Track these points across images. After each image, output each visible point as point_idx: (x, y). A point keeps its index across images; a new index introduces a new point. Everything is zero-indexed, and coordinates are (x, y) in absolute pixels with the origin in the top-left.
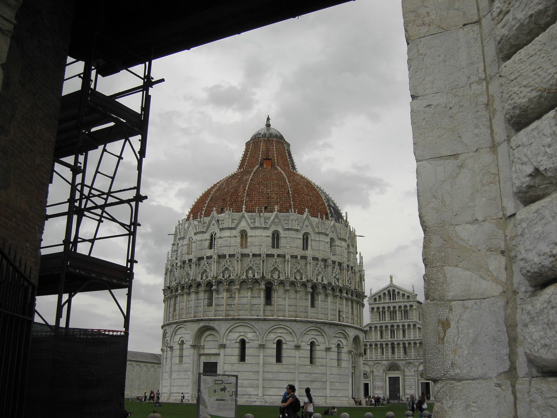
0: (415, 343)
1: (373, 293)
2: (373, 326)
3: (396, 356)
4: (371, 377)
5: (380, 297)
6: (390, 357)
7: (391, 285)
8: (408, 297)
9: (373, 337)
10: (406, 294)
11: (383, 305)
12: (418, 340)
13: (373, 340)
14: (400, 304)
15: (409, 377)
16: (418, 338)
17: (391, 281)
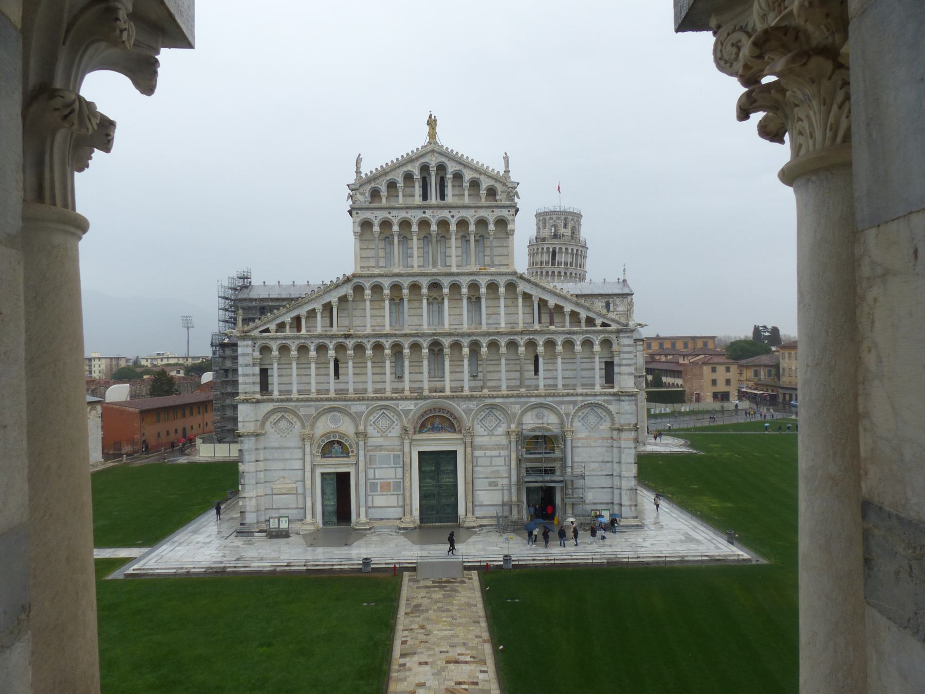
0: (512, 345)
1: (367, 169)
2: (367, 284)
3: (448, 385)
4: (361, 453)
5: (392, 185)
6: (426, 386)
7: (432, 146)
8: (492, 192)
9: (369, 322)
10: (485, 183)
11: (403, 214)
12: (522, 333)
13: (368, 331)
14: (464, 213)
15: (488, 453)
16: (520, 327)
17: (432, 134)
